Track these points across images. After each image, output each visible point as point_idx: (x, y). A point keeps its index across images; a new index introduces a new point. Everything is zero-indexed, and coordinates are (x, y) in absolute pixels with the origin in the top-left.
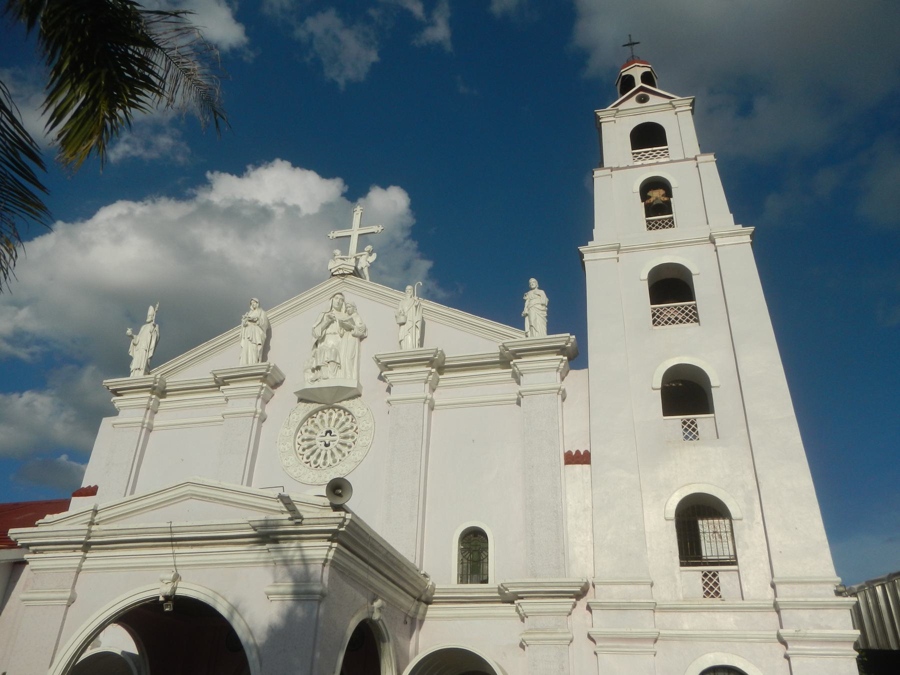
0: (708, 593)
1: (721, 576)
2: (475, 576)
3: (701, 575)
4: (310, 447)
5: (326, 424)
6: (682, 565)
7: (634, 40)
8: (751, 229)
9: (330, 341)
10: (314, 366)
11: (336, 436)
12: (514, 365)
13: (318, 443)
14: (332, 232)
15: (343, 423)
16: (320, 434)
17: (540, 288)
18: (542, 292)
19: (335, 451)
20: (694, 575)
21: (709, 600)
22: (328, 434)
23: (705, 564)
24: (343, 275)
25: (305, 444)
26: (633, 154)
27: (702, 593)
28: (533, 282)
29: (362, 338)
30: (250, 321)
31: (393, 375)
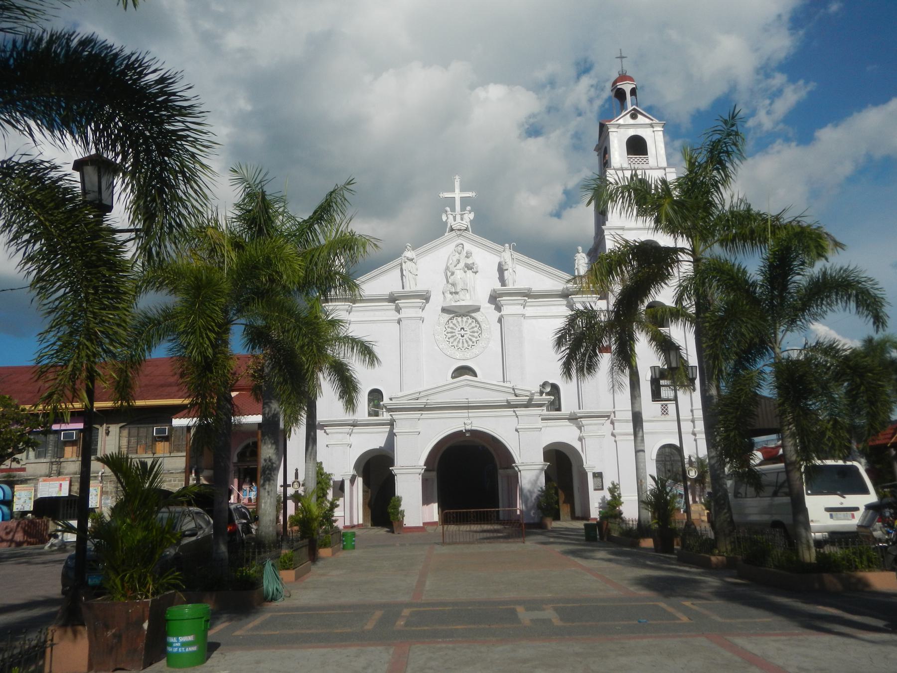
0: (663, 413)
1: (668, 405)
2: (552, 406)
3: (660, 405)
4: (453, 337)
5: (460, 324)
6: (653, 401)
7: (623, 55)
9: (459, 274)
10: (454, 291)
12: (572, 298)
13: (458, 335)
15: (470, 324)
16: (457, 330)
17: (583, 252)
18: (584, 255)
19: (468, 339)
20: (658, 405)
21: (663, 417)
23: (662, 401)
24: (459, 230)
25: (449, 335)
27: (661, 413)
28: (580, 248)
29: (476, 273)
30: (407, 259)
31: (503, 300)
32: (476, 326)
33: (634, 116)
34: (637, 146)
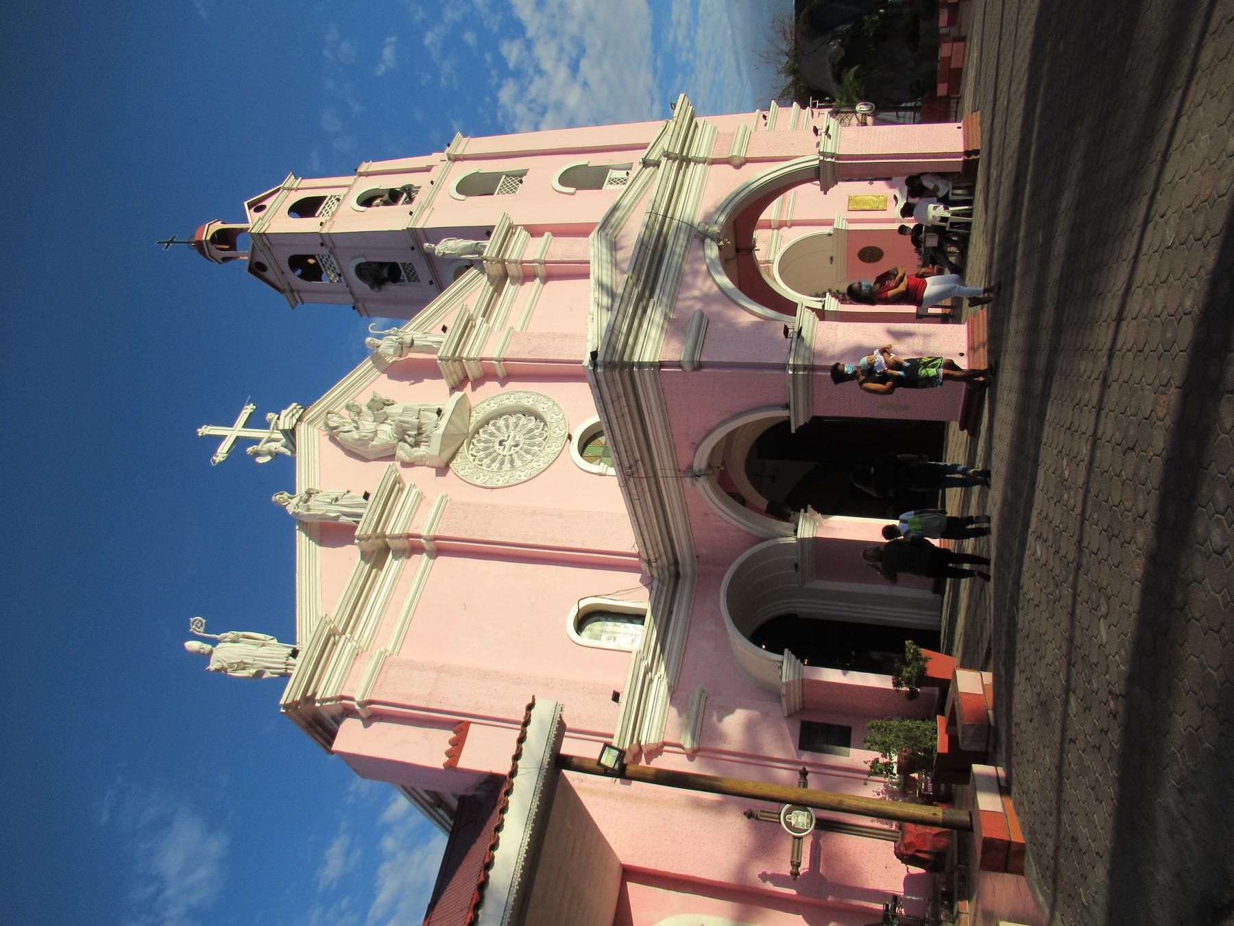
8: (459, 135)
11: (509, 436)
13: (512, 452)
14: (215, 458)
22: (504, 443)
24: (300, 419)
26: (318, 216)
30: (306, 501)
32: (506, 420)
33: (260, 209)
34: (306, 208)
